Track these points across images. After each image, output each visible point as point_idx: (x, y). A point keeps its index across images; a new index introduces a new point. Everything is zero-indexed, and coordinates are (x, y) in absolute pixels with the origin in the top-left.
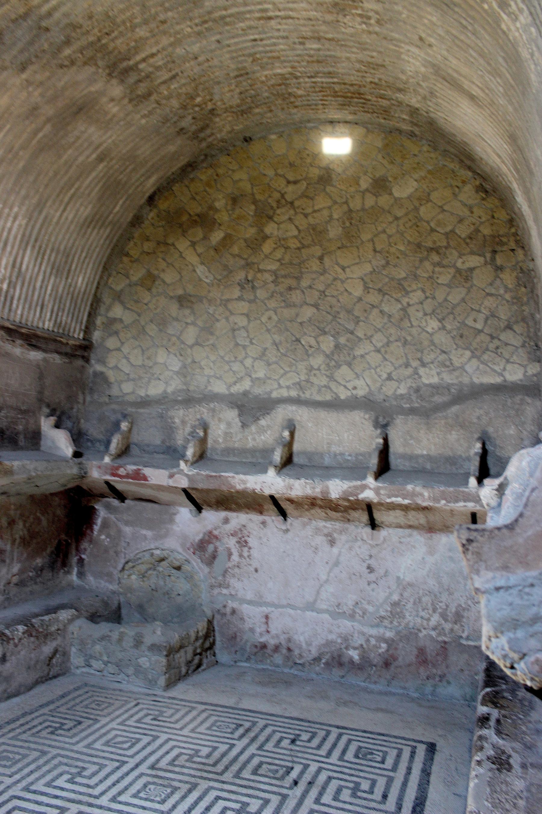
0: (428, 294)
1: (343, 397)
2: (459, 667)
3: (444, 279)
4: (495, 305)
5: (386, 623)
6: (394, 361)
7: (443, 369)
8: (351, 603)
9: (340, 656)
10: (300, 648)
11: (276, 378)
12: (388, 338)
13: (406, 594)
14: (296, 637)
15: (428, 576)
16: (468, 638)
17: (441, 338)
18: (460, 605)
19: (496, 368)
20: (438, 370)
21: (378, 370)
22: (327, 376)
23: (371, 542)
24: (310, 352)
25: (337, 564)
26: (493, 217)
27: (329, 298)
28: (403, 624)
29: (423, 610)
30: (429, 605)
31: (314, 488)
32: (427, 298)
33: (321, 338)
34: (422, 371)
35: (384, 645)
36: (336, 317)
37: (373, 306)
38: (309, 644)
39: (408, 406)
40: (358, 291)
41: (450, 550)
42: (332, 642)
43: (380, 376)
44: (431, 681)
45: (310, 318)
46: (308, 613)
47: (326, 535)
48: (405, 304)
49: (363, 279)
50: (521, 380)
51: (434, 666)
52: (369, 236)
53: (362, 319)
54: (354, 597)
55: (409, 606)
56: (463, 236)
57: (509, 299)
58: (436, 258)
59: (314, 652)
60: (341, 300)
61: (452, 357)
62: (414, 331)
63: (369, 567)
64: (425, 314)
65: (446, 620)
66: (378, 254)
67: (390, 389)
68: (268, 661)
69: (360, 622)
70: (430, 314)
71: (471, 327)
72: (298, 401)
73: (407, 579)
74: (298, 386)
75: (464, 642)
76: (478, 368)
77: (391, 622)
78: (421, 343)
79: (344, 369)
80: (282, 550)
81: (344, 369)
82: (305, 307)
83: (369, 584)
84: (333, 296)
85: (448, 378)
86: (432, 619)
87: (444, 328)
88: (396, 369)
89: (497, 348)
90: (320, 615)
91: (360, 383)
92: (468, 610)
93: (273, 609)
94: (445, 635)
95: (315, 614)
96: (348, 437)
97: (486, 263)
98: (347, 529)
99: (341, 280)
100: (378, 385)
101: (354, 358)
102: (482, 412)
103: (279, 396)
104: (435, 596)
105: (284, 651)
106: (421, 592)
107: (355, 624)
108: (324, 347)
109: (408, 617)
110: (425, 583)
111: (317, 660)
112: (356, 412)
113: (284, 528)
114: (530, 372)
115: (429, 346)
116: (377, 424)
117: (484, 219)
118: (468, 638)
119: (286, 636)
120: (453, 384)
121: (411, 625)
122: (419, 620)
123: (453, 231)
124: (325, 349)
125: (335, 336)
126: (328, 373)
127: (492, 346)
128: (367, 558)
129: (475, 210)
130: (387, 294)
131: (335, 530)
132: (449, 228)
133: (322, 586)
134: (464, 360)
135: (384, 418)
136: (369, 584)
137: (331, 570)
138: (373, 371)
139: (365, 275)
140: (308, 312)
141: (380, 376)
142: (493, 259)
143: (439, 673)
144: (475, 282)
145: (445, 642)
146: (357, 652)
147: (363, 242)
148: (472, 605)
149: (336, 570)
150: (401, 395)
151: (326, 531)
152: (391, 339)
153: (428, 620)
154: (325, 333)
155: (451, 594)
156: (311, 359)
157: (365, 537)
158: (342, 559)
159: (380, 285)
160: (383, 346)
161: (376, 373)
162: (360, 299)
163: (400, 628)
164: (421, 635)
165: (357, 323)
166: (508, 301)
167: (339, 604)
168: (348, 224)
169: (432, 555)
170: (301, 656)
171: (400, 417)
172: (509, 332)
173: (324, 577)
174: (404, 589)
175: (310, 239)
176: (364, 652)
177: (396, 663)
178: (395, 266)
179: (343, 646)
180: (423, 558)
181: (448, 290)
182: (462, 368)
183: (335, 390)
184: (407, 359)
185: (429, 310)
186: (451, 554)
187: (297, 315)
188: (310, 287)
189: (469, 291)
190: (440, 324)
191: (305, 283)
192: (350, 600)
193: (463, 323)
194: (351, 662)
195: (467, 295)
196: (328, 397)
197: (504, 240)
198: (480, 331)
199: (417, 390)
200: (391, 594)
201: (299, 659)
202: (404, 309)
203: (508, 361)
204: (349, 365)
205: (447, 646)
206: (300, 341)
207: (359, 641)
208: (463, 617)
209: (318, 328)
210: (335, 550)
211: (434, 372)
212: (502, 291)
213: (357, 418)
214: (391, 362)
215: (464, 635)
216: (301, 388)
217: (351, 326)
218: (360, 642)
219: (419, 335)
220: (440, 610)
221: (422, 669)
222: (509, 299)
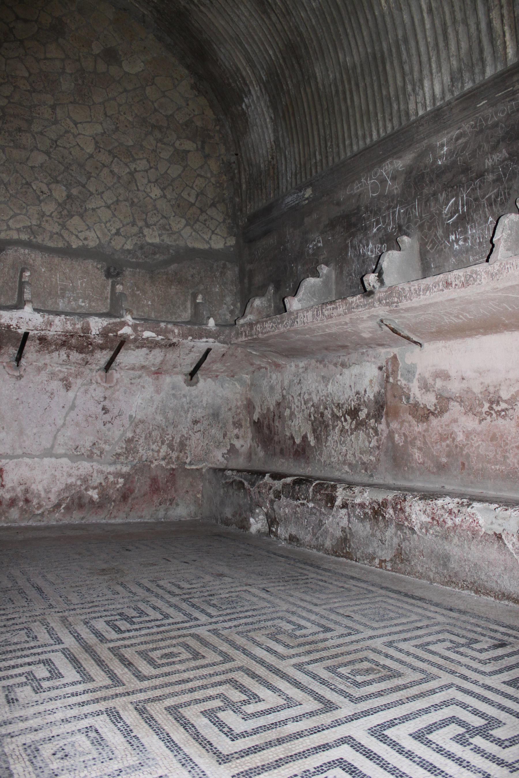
0: (152, 165)
1: (74, 247)
2: (185, 490)
3: (165, 155)
4: (204, 185)
5: (122, 458)
6: (122, 218)
7: (164, 232)
8: (88, 444)
9: (80, 498)
10: (39, 496)
11: (5, 218)
12: (117, 197)
13: (138, 431)
14: (33, 486)
15: (156, 413)
16: (191, 464)
17: (162, 204)
18: (183, 436)
19: (205, 237)
20: (160, 232)
21: (108, 225)
22: (59, 224)
23: (105, 384)
24: (42, 198)
25: (73, 407)
26: (203, 113)
27: (60, 148)
28: (137, 458)
29: (153, 443)
30: (158, 438)
31: (75, 324)
32: (151, 168)
33: (53, 186)
34: (146, 231)
35: (121, 480)
36: (68, 168)
37: (104, 166)
38: (48, 491)
39: (134, 260)
40: (90, 149)
41: (173, 389)
42: (71, 485)
43: (109, 231)
44: (163, 506)
45: (42, 164)
46: (45, 460)
47: (62, 380)
48: (133, 169)
49: (94, 139)
50: (222, 249)
51: (165, 491)
52: (101, 100)
53: (93, 174)
54: (91, 438)
55: (141, 441)
56: (181, 122)
57: (214, 183)
58: (159, 136)
59: (54, 499)
60: (73, 153)
61: (171, 222)
62: (140, 194)
63: (103, 409)
64: (149, 182)
65: (173, 450)
66: (108, 118)
67: (118, 243)
68: (3, 518)
69: (98, 462)
70: (154, 182)
71: (186, 200)
72: (28, 245)
73: (139, 417)
74: (29, 230)
75: (188, 467)
76: (191, 235)
77: (127, 458)
78: (146, 206)
79: (76, 220)
80: (15, 398)
81: (76, 220)
82: (35, 153)
83: (104, 425)
84: (65, 148)
85: (168, 241)
86: (162, 450)
87: (165, 196)
88: (123, 226)
89: (205, 220)
90: (59, 460)
91: (91, 234)
92: (190, 439)
93: (8, 460)
94: (173, 463)
95: (53, 460)
96: (82, 284)
97: (197, 150)
98: (82, 373)
99: (73, 134)
100: (108, 239)
101: (86, 210)
102: (194, 271)
103: (8, 238)
104: (163, 429)
105: (21, 504)
106: (151, 427)
107: (94, 463)
108: (56, 194)
109: (140, 451)
110: (155, 419)
111: (58, 506)
112: (90, 261)
113: (17, 374)
114: (228, 244)
115: (152, 210)
116: (108, 275)
117: (196, 113)
118: (191, 464)
119: (23, 487)
120: (171, 246)
121: (144, 458)
122: (151, 453)
123: (172, 115)
124: (57, 197)
125: (68, 186)
126: (60, 221)
127: (202, 218)
128: (102, 400)
129: (190, 103)
130: (116, 156)
131: (70, 374)
132: (170, 112)
133: (59, 430)
134: (181, 225)
135: (115, 269)
136: (104, 425)
137: (67, 414)
138: (103, 224)
139: (97, 135)
140: (39, 158)
141: (109, 231)
142: (203, 148)
143: (169, 497)
144: (189, 163)
145: (173, 469)
146: (96, 491)
147: (94, 103)
148: (193, 435)
149: (73, 414)
150: (128, 250)
151: (61, 376)
152: (120, 198)
153: (158, 451)
154: (58, 182)
155: (175, 427)
156: (42, 204)
157: (99, 381)
158: (78, 402)
159: (110, 148)
160: (113, 204)
161: (106, 227)
162: (91, 156)
163: (135, 462)
164: (153, 466)
165: (89, 178)
166: (213, 184)
167: (77, 447)
168: (80, 82)
169: (159, 394)
170: (40, 506)
171: (129, 269)
172: (214, 209)
173: (60, 422)
174: (136, 425)
175: (43, 86)
176: (103, 490)
177: (133, 496)
178: (124, 133)
179: (83, 488)
180: (152, 397)
181: (168, 165)
182: (179, 232)
183: (67, 239)
184: (134, 219)
185: (153, 180)
186: (174, 392)
187: (28, 159)
188: (41, 133)
189: (184, 170)
190: (162, 193)
191: (36, 128)
192: (87, 441)
193: (179, 195)
194: (91, 501)
195: (182, 172)
196: (60, 245)
197: (212, 134)
198: (193, 205)
199: (141, 248)
200: (125, 432)
201: (38, 509)
202: (131, 173)
203: (213, 232)
204: (81, 216)
205: (175, 472)
206: (31, 186)
207: (97, 479)
208: (186, 445)
209: (50, 175)
210: (71, 394)
211: (156, 233)
212: (209, 175)
213: (90, 267)
214: (120, 219)
215: (188, 461)
216: (33, 233)
217: (83, 180)
218: (99, 481)
219: (144, 198)
220: (167, 442)
221: (155, 498)
222: (214, 183)
